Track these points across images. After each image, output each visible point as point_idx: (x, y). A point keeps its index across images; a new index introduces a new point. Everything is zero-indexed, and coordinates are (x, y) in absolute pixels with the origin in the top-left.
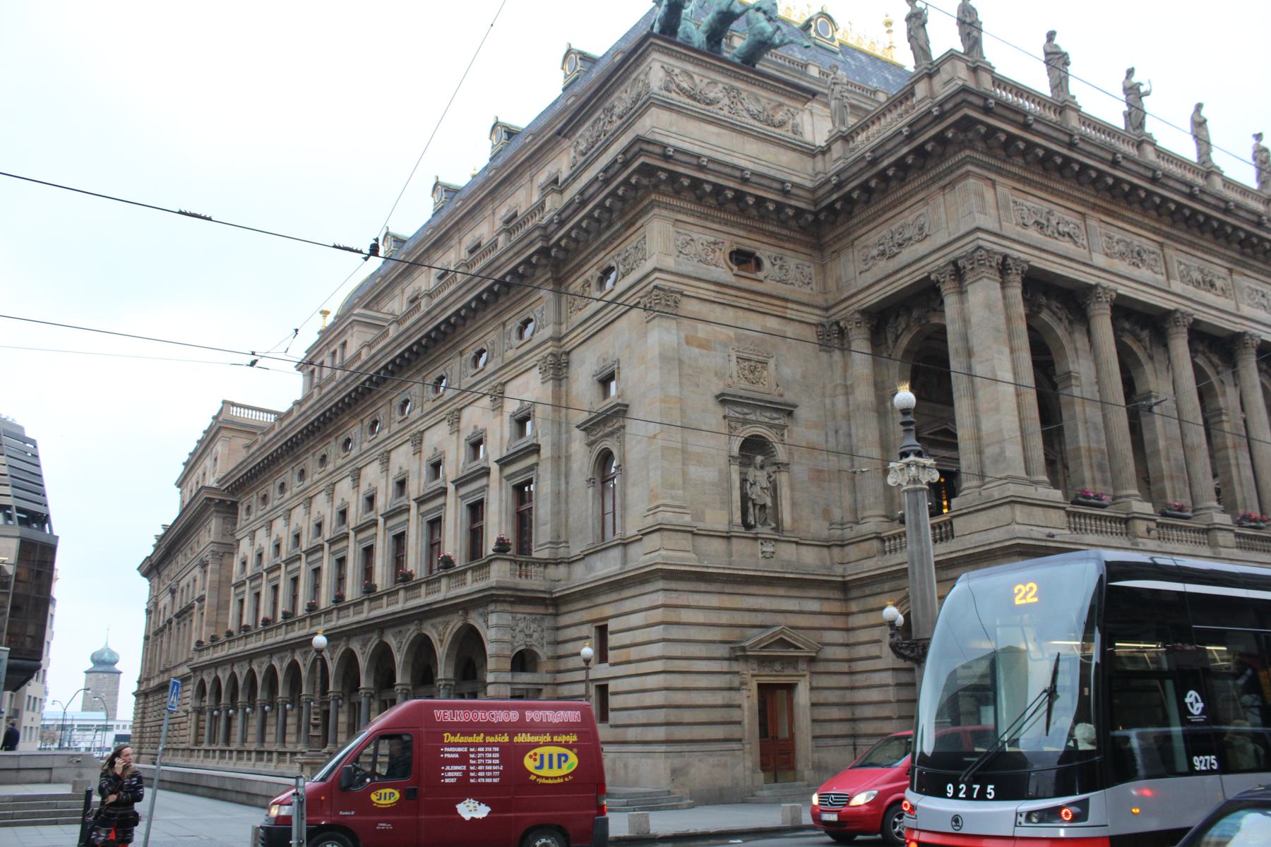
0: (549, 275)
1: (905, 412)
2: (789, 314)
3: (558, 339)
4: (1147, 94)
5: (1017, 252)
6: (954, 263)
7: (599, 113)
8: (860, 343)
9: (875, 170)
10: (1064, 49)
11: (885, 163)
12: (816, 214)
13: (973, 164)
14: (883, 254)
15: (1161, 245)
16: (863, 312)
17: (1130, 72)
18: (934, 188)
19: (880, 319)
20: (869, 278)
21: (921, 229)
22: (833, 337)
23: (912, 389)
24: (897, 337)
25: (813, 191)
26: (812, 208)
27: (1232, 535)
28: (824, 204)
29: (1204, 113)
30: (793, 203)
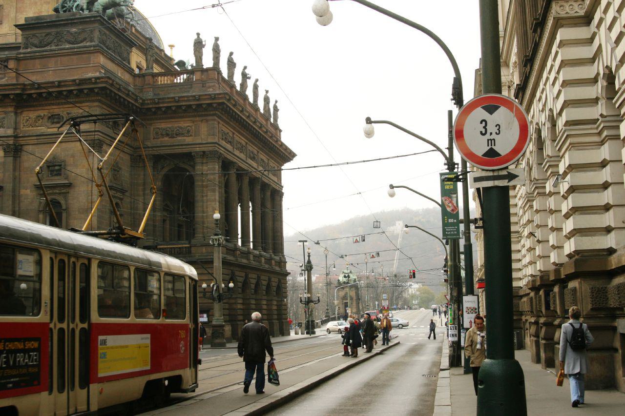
0: (15, 104)
1: (217, 220)
2: (126, 150)
3: (16, 137)
4: (249, 78)
5: (222, 151)
6: (204, 152)
7: (53, 31)
8: (149, 165)
9: (176, 104)
10: (235, 61)
11: (184, 104)
12: (140, 109)
13: (216, 116)
14: (167, 135)
15: (247, 143)
16: (154, 155)
17: (245, 68)
18: (197, 119)
19: (157, 159)
20: (158, 142)
21: (188, 131)
22: (137, 160)
23: (220, 213)
24: (163, 168)
25: (144, 100)
26: (140, 107)
27: (225, 249)
28: (146, 107)
29: (258, 83)
30: (137, 104)
